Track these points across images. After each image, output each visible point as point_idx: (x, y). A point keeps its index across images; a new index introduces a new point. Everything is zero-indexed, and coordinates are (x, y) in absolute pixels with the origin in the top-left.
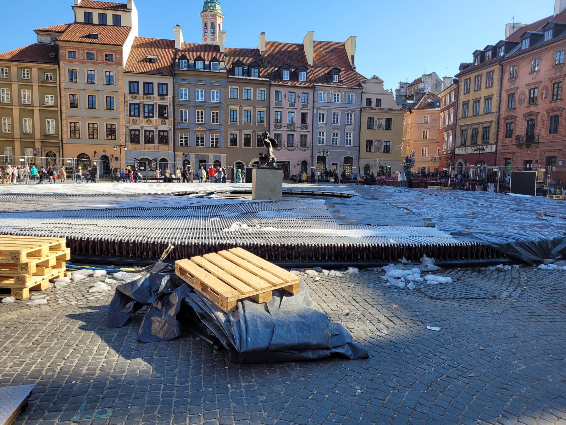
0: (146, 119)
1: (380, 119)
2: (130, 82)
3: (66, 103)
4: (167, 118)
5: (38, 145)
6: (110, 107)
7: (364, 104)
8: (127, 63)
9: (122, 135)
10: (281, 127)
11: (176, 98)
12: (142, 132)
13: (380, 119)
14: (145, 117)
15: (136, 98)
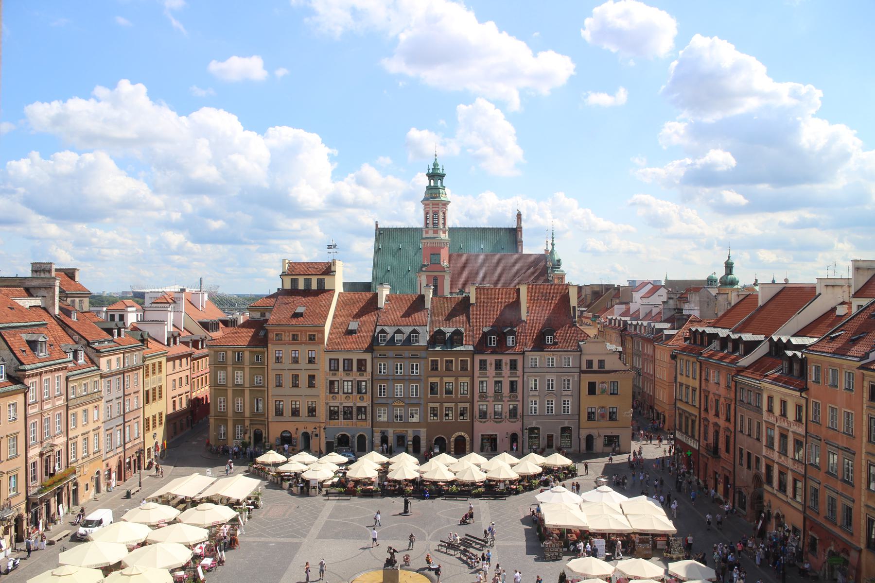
0: (345, 396)
1: (603, 383)
2: (330, 360)
3: (272, 382)
4: (365, 393)
5: (247, 423)
6: (311, 385)
7: (584, 367)
8: (331, 334)
9: (322, 412)
10: (487, 397)
11: (375, 373)
12: (341, 408)
13: (603, 383)
14: (344, 393)
15: (335, 375)
